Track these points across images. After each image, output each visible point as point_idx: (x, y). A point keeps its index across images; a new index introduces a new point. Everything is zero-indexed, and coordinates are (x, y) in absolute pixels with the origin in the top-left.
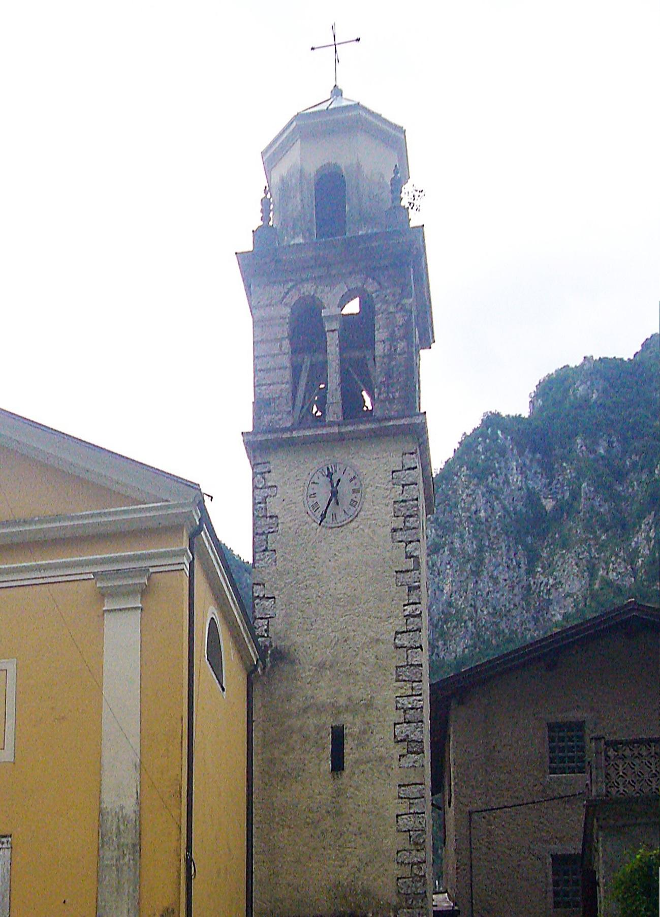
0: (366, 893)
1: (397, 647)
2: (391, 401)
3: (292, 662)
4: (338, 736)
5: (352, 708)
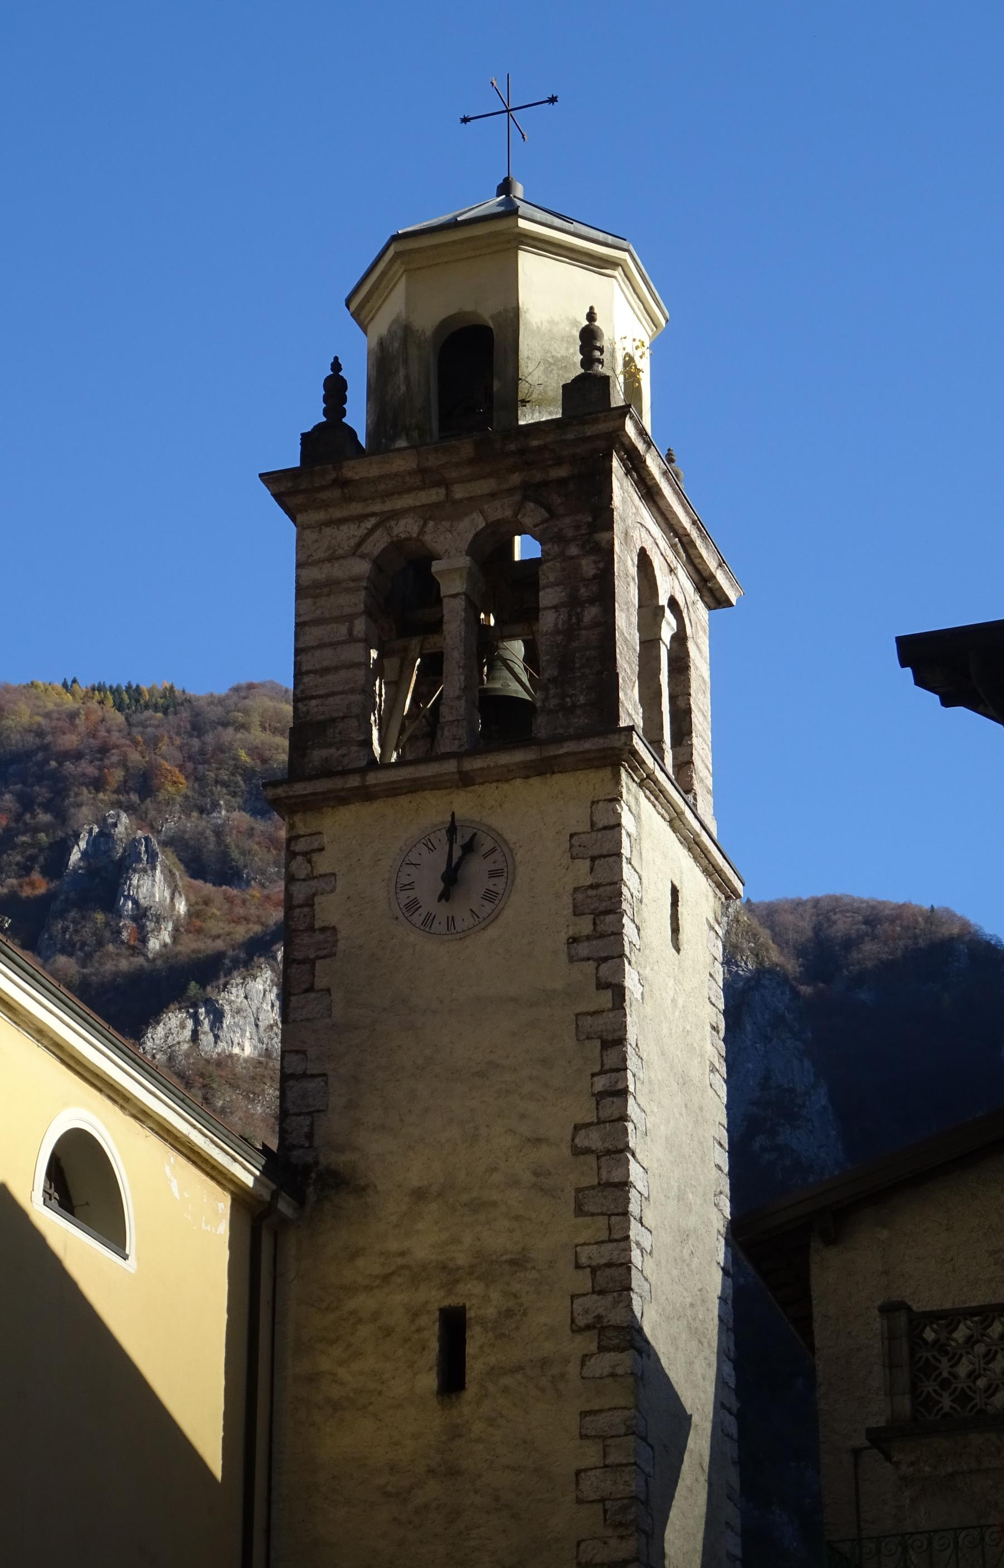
1: (578, 1152)
3: (361, 1190)
4: (454, 1325)
5: (487, 1268)
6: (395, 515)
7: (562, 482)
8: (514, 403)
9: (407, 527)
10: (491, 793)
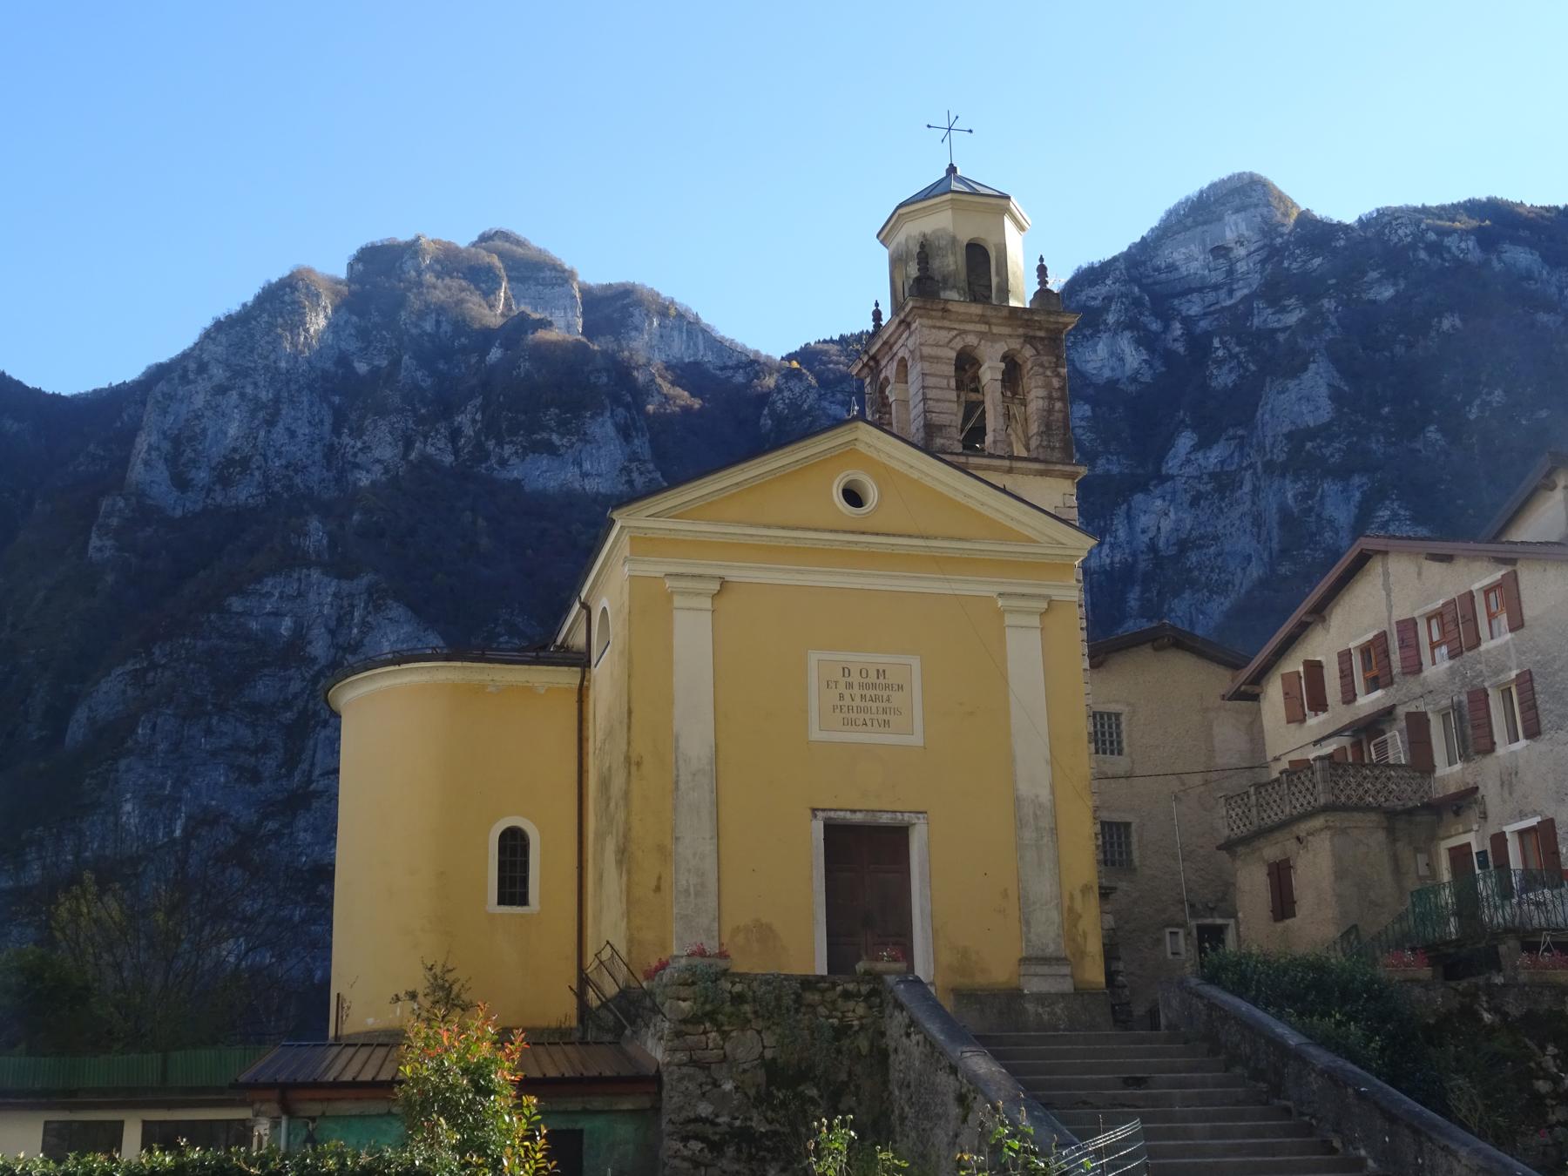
2: (1053, 449)
6: (963, 332)
7: (1042, 339)
8: (1004, 291)
9: (972, 340)
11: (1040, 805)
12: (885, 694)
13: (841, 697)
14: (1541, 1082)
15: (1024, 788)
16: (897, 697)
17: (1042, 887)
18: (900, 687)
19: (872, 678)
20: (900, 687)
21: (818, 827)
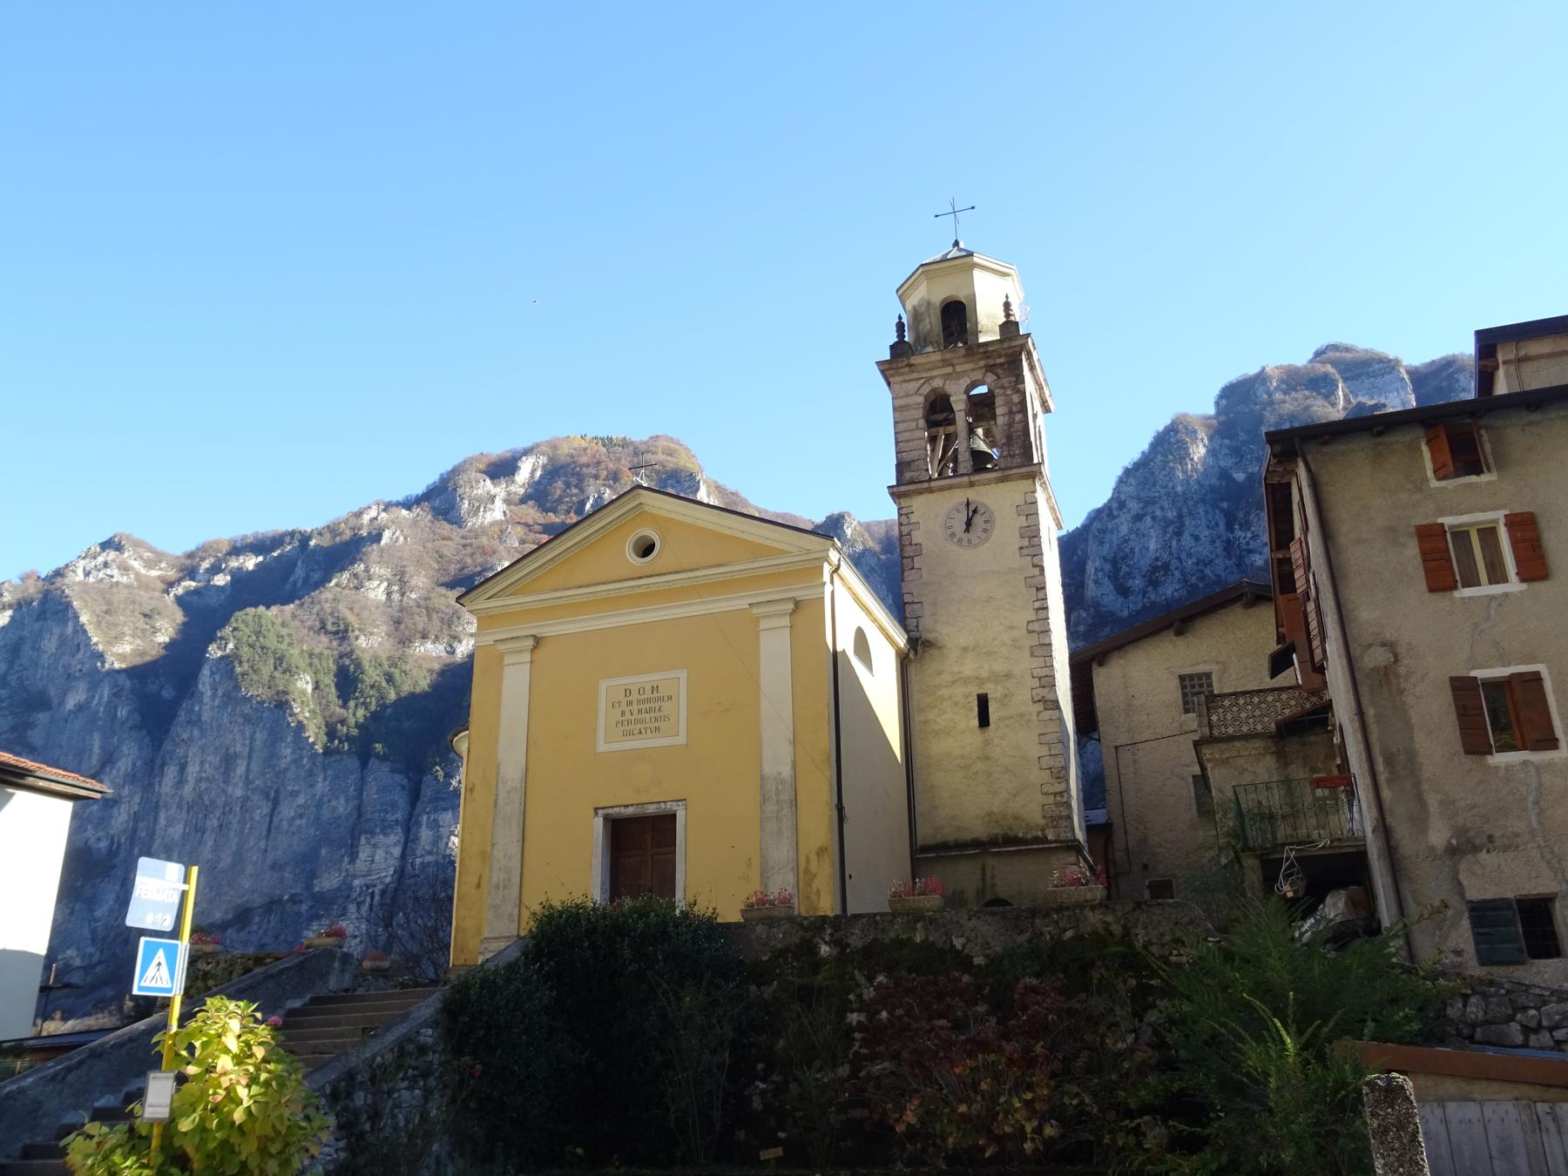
0: (1015, 818)
1: (1030, 632)
3: (940, 648)
4: (983, 702)
5: (995, 678)
6: (929, 379)
8: (976, 333)
9: (938, 383)
10: (982, 489)
11: (782, 782)
12: (657, 705)
13: (623, 713)
14: (855, 1015)
15: (769, 768)
16: (666, 706)
17: (781, 853)
18: (670, 698)
19: (648, 694)
20: (670, 698)
21: (599, 822)
